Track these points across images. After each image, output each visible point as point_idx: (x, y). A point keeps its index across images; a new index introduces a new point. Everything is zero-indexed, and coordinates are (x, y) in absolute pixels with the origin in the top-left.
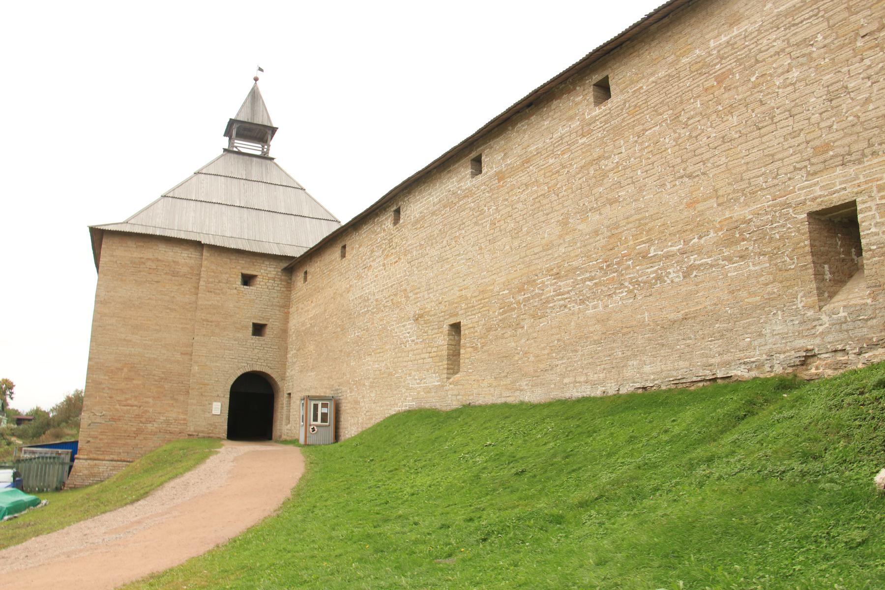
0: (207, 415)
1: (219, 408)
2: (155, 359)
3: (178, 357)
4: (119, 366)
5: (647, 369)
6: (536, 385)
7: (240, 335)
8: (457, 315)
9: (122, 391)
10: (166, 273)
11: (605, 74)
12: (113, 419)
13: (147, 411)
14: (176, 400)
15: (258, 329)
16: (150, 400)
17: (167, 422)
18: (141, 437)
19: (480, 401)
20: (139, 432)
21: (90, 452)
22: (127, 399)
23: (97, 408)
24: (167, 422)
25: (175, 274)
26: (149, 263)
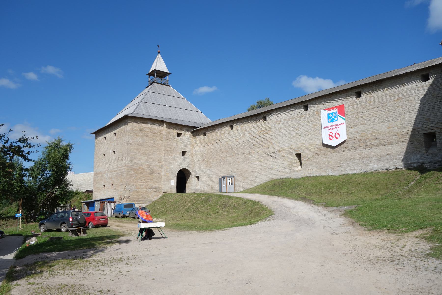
0: (170, 185)
1: (174, 182)
2: (150, 165)
3: (158, 164)
4: (138, 168)
5: (375, 166)
6: (335, 170)
7: (178, 155)
8: (299, 151)
9: (140, 178)
10: (152, 133)
11: (359, 90)
12: (137, 188)
13: (148, 185)
14: (158, 180)
15: (184, 153)
16: (149, 180)
17: (156, 188)
18: (147, 194)
19: (312, 175)
20: (146, 192)
21: (130, 201)
22: (141, 180)
23: (131, 184)
24: (156, 188)
25: (154, 133)
26: (145, 129)
